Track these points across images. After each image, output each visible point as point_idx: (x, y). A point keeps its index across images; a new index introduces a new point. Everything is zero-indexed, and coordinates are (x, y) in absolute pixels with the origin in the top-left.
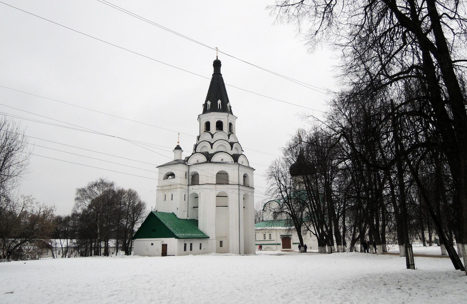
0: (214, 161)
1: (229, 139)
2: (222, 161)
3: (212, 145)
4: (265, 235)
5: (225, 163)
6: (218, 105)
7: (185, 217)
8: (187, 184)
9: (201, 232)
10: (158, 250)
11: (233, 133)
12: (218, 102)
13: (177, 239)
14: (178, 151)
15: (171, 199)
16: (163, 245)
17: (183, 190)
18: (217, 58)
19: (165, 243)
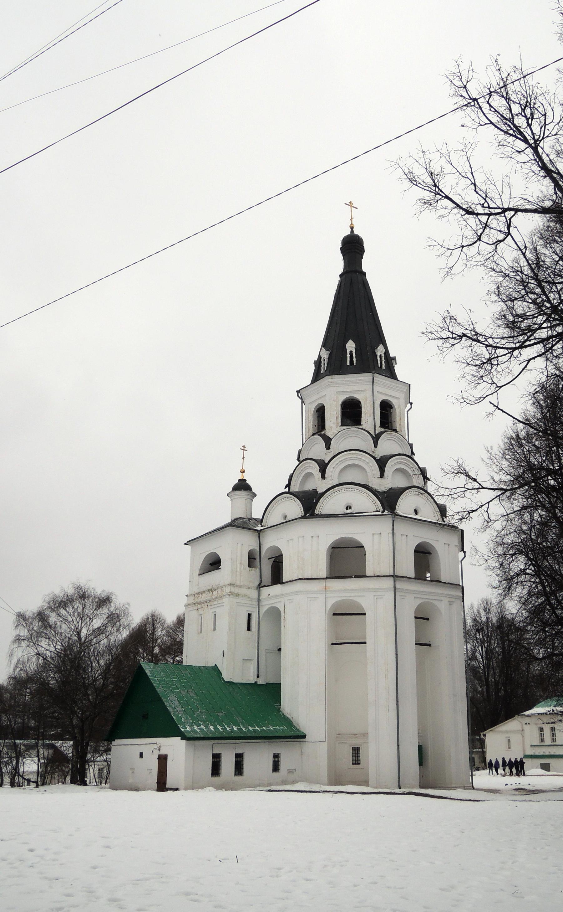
0: (324, 512)
1: (376, 446)
2: (349, 511)
4: (541, 729)
5: (361, 515)
6: (348, 356)
7: (251, 679)
8: (257, 583)
9: (288, 722)
10: (150, 770)
11: (395, 431)
12: (347, 346)
13: (185, 741)
14: (242, 494)
15: (212, 627)
17: (240, 600)
18: (352, 231)
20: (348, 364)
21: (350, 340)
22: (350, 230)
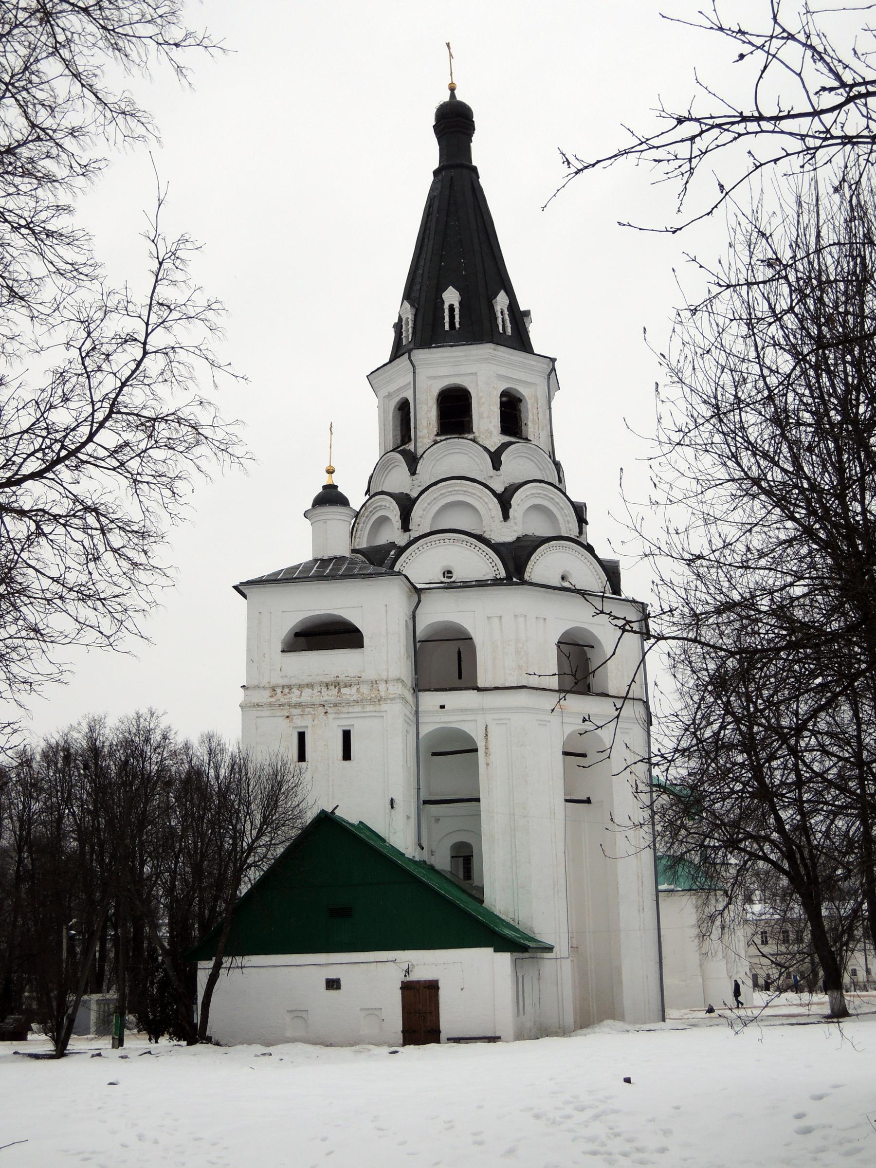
3: (505, 500)
10: (373, 1012)
13: (509, 954)
16: (408, 988)
19: (420, 975)
20: (447, 327)
21: (451, 287)
22: (448, 93)
